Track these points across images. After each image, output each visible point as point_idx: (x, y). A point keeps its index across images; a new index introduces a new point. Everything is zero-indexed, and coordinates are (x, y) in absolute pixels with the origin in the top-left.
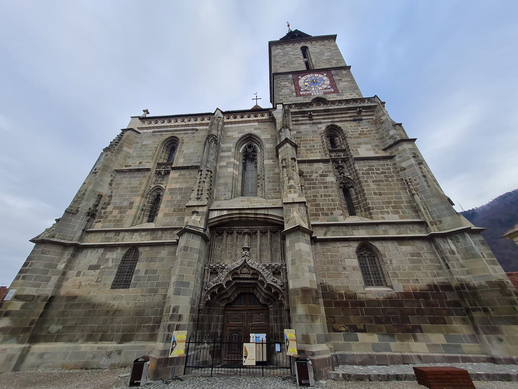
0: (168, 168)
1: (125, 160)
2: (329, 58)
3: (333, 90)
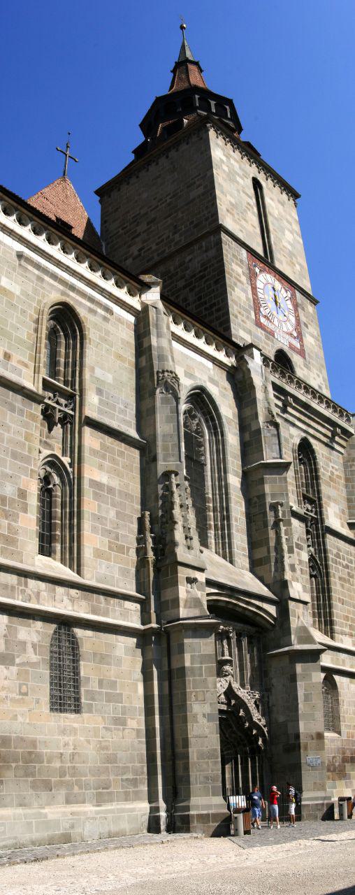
2: (289, 247)
3: (298, 346)
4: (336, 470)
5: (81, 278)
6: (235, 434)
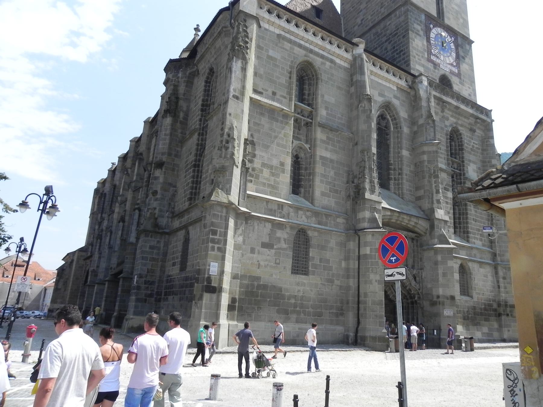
2: (456, 8)
3: (456, 71)
4: (476, 144)
5: (317, 45)
6: (408, 127)
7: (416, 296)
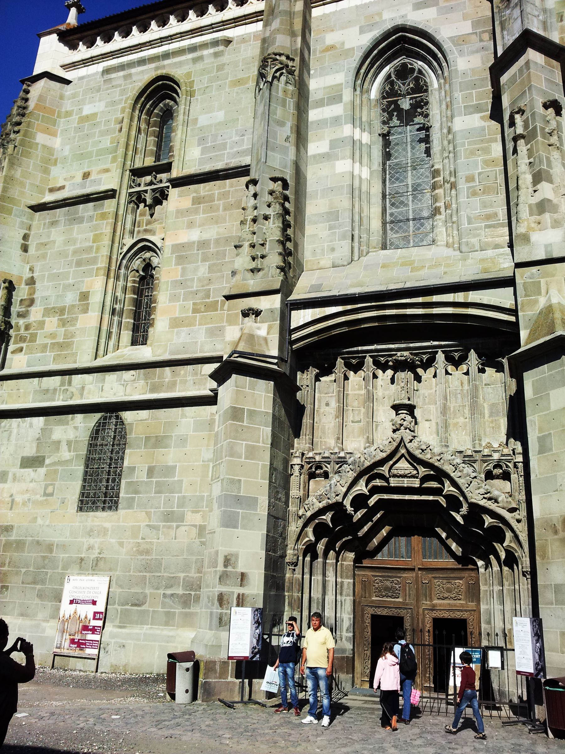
0: (161, 181)
1: (46, 171)
7: (509, 535)
